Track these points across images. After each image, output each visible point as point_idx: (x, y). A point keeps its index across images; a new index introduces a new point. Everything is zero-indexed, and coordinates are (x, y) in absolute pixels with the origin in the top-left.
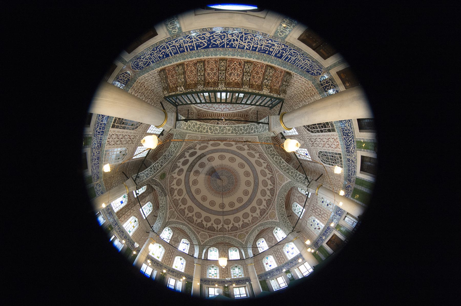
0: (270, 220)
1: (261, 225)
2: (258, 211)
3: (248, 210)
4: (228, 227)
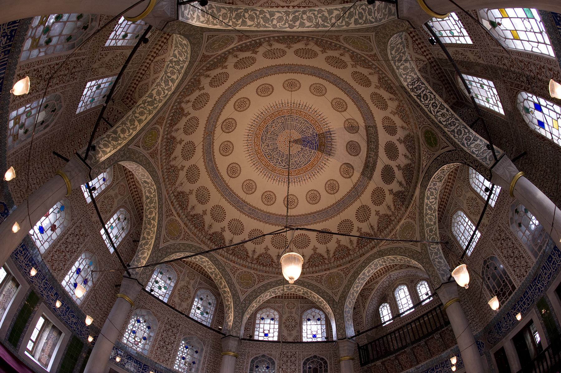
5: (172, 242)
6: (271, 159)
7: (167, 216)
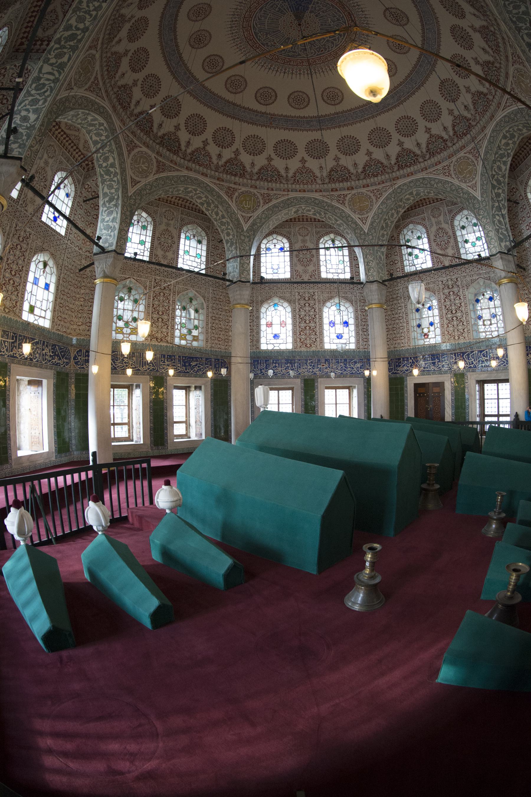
0: (347, 210)
4: (220, 156)
5: (371, 215)
7: (343, 203)
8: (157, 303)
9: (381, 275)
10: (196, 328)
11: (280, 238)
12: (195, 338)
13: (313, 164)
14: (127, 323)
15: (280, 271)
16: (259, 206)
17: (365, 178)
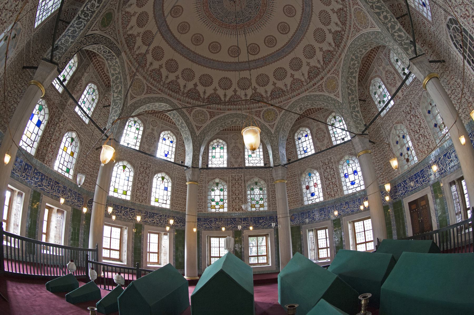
1: (308, 98)
2: (305, 69)
3: (284, 63)
5: (340, 89)
6: (258, 5)
8: (234, 189)
9: (360, 128)
10: (261, 199)
11: (304, 129)
12: (262, 206)
13: (297, 75)
14: (217, 203)
15: (309, 150)
16: (277, 115)
17: (326, 67)
